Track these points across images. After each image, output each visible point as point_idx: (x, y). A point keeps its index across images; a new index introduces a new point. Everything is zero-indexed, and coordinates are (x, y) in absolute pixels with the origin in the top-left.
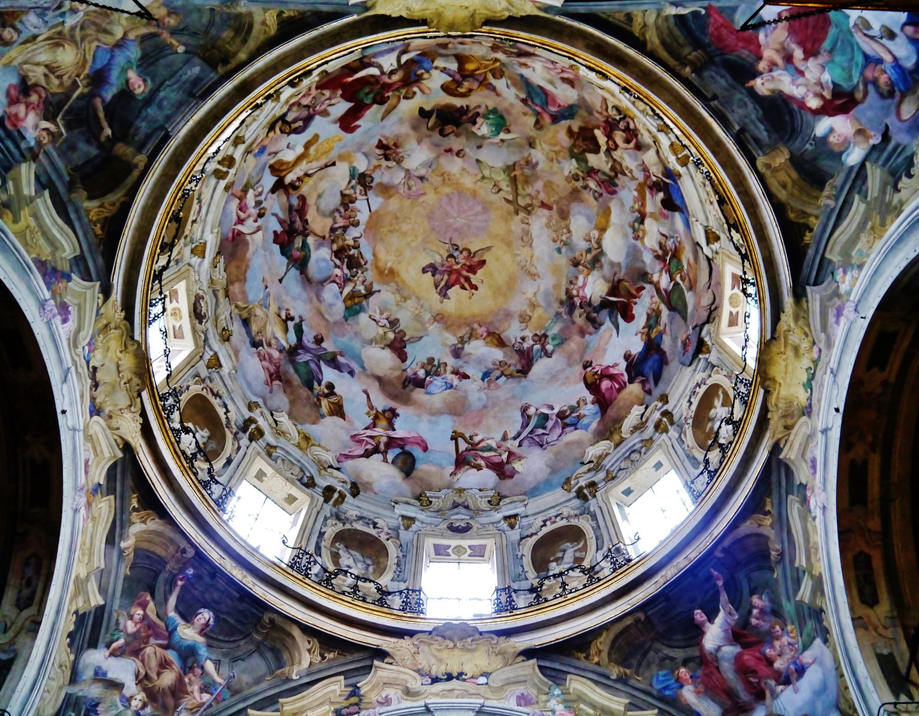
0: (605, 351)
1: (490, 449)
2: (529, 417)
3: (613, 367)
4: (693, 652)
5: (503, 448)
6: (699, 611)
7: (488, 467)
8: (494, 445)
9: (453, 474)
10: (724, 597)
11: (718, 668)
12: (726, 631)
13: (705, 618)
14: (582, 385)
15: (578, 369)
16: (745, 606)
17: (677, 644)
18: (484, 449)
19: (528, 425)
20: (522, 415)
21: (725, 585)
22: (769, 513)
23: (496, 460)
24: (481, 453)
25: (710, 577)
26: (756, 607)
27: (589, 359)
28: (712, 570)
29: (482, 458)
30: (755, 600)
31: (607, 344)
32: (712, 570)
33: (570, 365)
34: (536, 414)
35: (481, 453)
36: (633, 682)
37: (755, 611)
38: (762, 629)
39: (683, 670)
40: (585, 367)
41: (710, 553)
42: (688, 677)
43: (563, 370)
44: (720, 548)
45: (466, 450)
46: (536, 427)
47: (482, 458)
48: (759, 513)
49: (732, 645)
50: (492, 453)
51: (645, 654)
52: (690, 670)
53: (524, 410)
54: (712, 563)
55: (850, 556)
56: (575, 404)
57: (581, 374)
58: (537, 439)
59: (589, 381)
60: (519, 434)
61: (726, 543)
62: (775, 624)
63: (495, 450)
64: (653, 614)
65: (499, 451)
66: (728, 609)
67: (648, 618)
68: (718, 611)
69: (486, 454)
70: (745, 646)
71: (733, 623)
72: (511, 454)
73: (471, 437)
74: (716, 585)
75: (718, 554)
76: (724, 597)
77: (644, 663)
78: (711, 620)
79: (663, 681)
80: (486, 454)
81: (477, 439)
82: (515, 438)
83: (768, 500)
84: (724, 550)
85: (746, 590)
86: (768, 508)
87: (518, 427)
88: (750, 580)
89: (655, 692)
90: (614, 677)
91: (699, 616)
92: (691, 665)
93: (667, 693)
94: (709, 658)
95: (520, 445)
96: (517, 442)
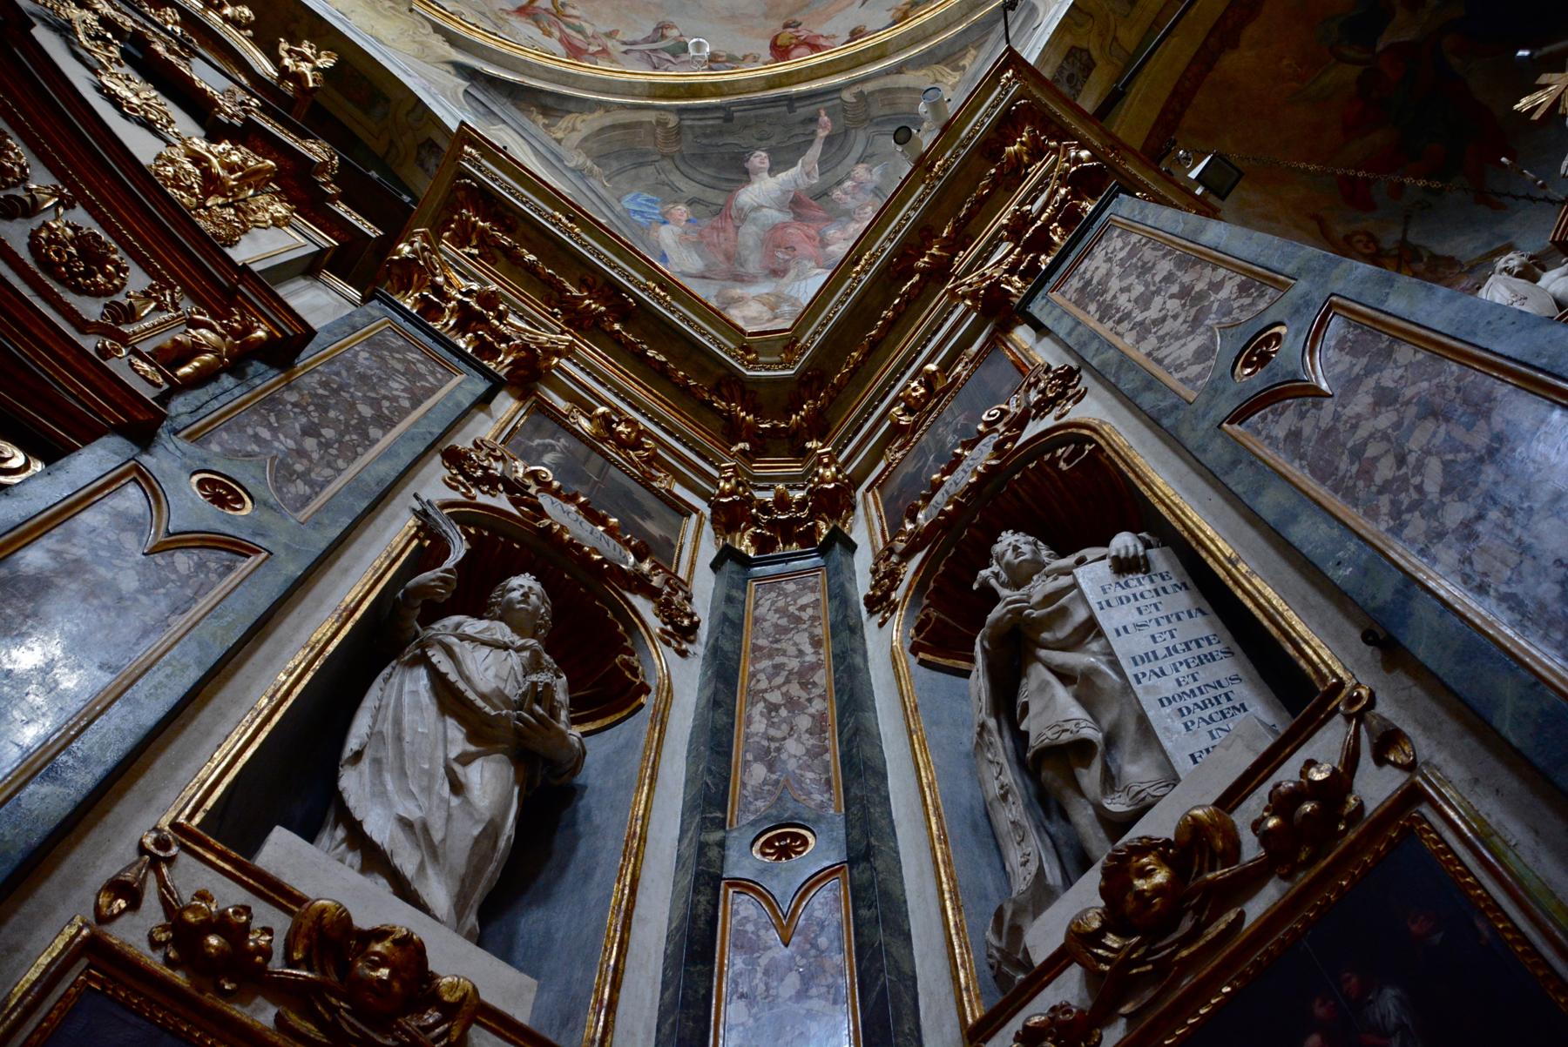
0: (829, 18)
1: (580, 31)
2: (663, 37)
3: (827, 38)
4: (718, 198)
5: (599, 42)
6: (764, 154)
7: (560, 40)
8: (589, 30)
9: (508, 13)
10: (815, 151)
11: (738, 227)
12: (785, 192)
13: (767, 164)
14: (768, 43)
15: (775, 26)
16: (840, 171)
17: (699, 177)
18: (568, 25)
19: (654, 42)
20: (656, 30)
21: (827, 137)
22: (964, 68)
23: (579, 44)
24: (563, 27)
25: (813, 120)
26: (853, 180)
27: (798, 18)
28: (823, 113)
29: (561, 30)
30: (860, 171)
31: (840, 10)
32: (823, 113)
33: (766, 16)
34: (675, 38)
35: (563, 27)
36: (594, 183)
37: (848, 184)
38: (842, 207)
39: (682, 208)
40: (786, 26)
41: (837, 89)
42: (684, 218)
43: (752, 17)
44: (855, 89)
45: (546, 10)
46: (665, 50)
47: (561, 30)
48: (946, 65)
49: (780, 210)
50: (580, 37)
51: (641, 165)
52: (692, 213)
53: (661, 30)
54: (829, 104)
55: (1068, 40)
56: (740, 55)
57: (775, 30)
58: (655, 60)
59: (779, 43)
60: (634, 43)
61: (868, 87)
62: (868, 205)
63: (586, 36)
64: (691, 127)
65: (591, 40)
66: (808, 168)
67: (679, 129)
68: (794, 164)
69: (568, 31)
70: (799, 217)
71: (803, 187)
72: (604, 52)
73: (563, 5)
74: (814, 133)
75: (847, 96)
76: (815, 151)
77: (633, 172)
78: (772, 171)
79: (640, 204)
80: (568, 31)
81: (569, 11)
82: (624, 43)
83: (973, 52)
84: (861, 96)
85: (858, 150)
86: (966, 62)
87: (639, 36)
88: (869, 142)
89: (618, 208)
90: (571, 165)
91: (759, 159)
92: (700, 207)
93: (637, 217)
94: (734, 213)
95: (625, 52)
96: (625, 48)
